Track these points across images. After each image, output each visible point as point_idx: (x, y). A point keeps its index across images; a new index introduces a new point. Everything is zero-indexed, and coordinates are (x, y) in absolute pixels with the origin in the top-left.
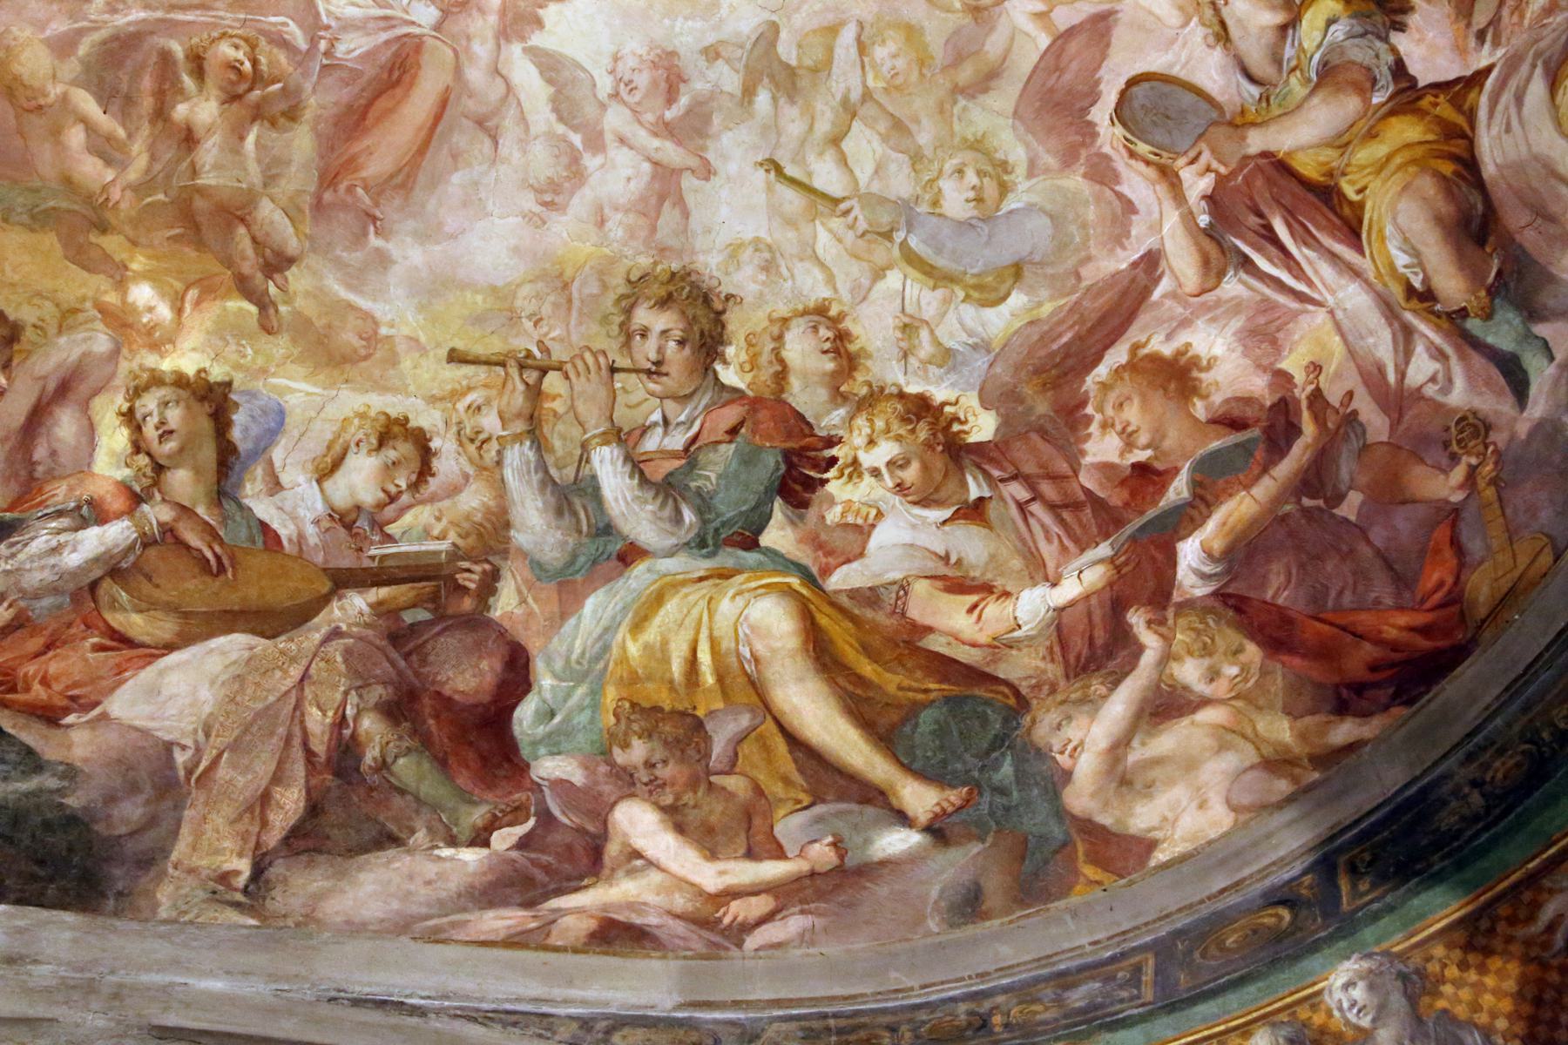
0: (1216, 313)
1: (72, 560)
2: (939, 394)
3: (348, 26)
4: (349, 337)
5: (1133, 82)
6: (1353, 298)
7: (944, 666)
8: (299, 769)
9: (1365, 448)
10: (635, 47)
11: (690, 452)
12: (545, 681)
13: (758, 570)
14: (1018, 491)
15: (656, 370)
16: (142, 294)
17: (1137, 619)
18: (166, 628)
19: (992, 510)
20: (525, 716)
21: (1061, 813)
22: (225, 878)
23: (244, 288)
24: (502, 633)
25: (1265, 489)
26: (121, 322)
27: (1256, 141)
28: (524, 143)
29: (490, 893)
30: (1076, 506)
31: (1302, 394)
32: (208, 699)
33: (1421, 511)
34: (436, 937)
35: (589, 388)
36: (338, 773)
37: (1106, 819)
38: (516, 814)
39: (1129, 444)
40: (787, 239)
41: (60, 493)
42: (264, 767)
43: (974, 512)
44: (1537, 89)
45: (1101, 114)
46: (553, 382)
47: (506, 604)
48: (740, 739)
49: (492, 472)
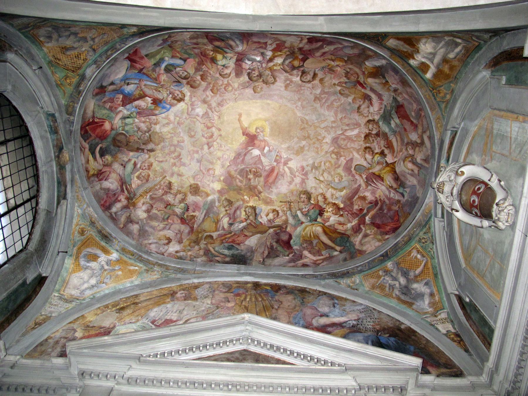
0: (368, 191)
1: (240, 227)
2: (336, 202)
3: (267, 166)
4: (269, 200)
5: (356, 165)
6: (383, 188)
7: (339, 233)
8: (267, 249)
9: (386, 205)
10: (299, 165)
11: (308, 211)
12: (294, 238)
13: (317, 224)
14: (346, 213)
15: (304, 202)
16: (246, 197)
17: (362, 226)
18: (251, 234)
19: (344, 215)
20: (292, 241)
21: (355, 249)
22: (260, 261)
23: (257, 196)
24: (288, 233)
25: (375, 210)
26: (243, 200)
27: (371, 171)
28: (287, 177)
29: (290, 262)
30: (353, 214)
31: (378, 199)
33: (393, 211)
34: (284, 266)
35: (296, 204)
36: (271, 249)
37: (360, 249)
38: (292, 253)
39: (359, 206)
40: (317, 186)
41: (238, 220)
42: (263, 249)
43: (342, 215)
44: (402, 163)
45: (353, 169)
46: (292, 204)
47: (288, 229)
49: (286, 214)
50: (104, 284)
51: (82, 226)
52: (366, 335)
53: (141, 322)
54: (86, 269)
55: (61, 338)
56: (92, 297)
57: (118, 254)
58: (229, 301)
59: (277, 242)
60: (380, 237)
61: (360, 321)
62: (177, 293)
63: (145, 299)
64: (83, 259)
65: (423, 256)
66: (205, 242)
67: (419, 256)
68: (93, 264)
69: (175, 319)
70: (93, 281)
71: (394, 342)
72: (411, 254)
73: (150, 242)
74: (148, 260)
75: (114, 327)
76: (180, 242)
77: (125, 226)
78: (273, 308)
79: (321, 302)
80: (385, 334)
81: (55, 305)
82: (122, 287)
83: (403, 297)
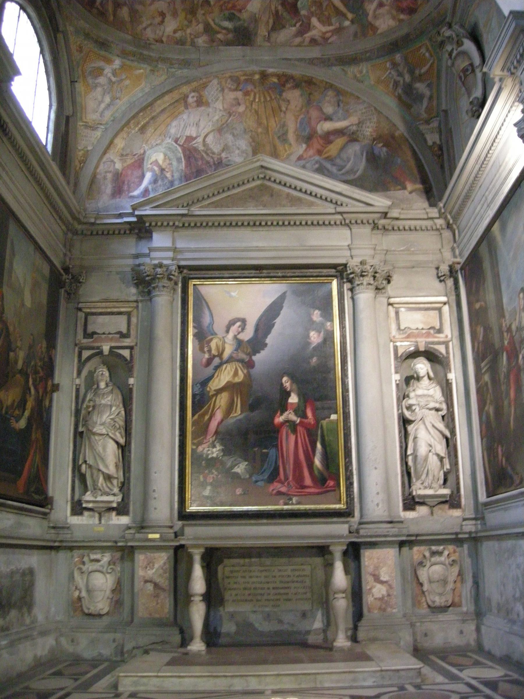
8: (272, 16)
21: (367, 21)
32: (259, 5)
37: (373, 23)
38: (300, 20)
42: (267, 17)
48: (327, 6)
50: (118, 101)
51: (79, 43)
52: (363, 144)
53: (166, 142)
54: (96, 86)
55: (106, 172)
56: (112, 119)
57: (120, 59)
58: (239, 104)
59: (283, 4)
60: (394, 12)
61: (360, 125)
62: (188, 97)
63: (160, 109)
64: (90, 77)
65: (431, 56)
66: (203, 12)
67: (427, 54)
68: (102, 80)
69: (194, 135)
70: (107, 99)
71: (385, 154)
72: (420, 50)
73: (144, 25)
74: (150, 56)
75: (145, 152)
76: (175, 14)
77: (114, 15)
78: (281, 111)
79: (327, 98)
80: (379, 143)
81: (86, 136)
82: (135, 99)
83: (404, 97)
